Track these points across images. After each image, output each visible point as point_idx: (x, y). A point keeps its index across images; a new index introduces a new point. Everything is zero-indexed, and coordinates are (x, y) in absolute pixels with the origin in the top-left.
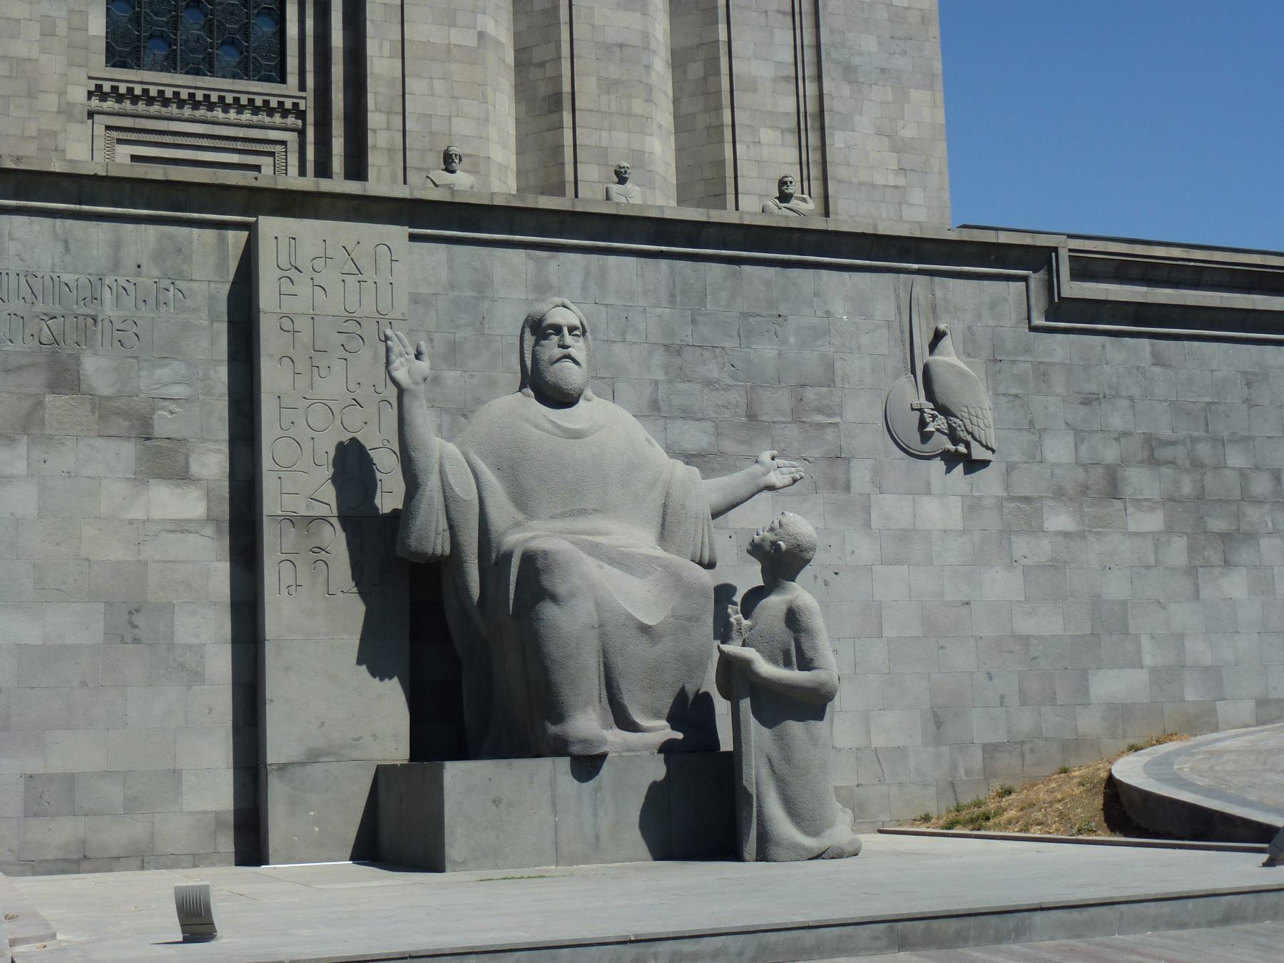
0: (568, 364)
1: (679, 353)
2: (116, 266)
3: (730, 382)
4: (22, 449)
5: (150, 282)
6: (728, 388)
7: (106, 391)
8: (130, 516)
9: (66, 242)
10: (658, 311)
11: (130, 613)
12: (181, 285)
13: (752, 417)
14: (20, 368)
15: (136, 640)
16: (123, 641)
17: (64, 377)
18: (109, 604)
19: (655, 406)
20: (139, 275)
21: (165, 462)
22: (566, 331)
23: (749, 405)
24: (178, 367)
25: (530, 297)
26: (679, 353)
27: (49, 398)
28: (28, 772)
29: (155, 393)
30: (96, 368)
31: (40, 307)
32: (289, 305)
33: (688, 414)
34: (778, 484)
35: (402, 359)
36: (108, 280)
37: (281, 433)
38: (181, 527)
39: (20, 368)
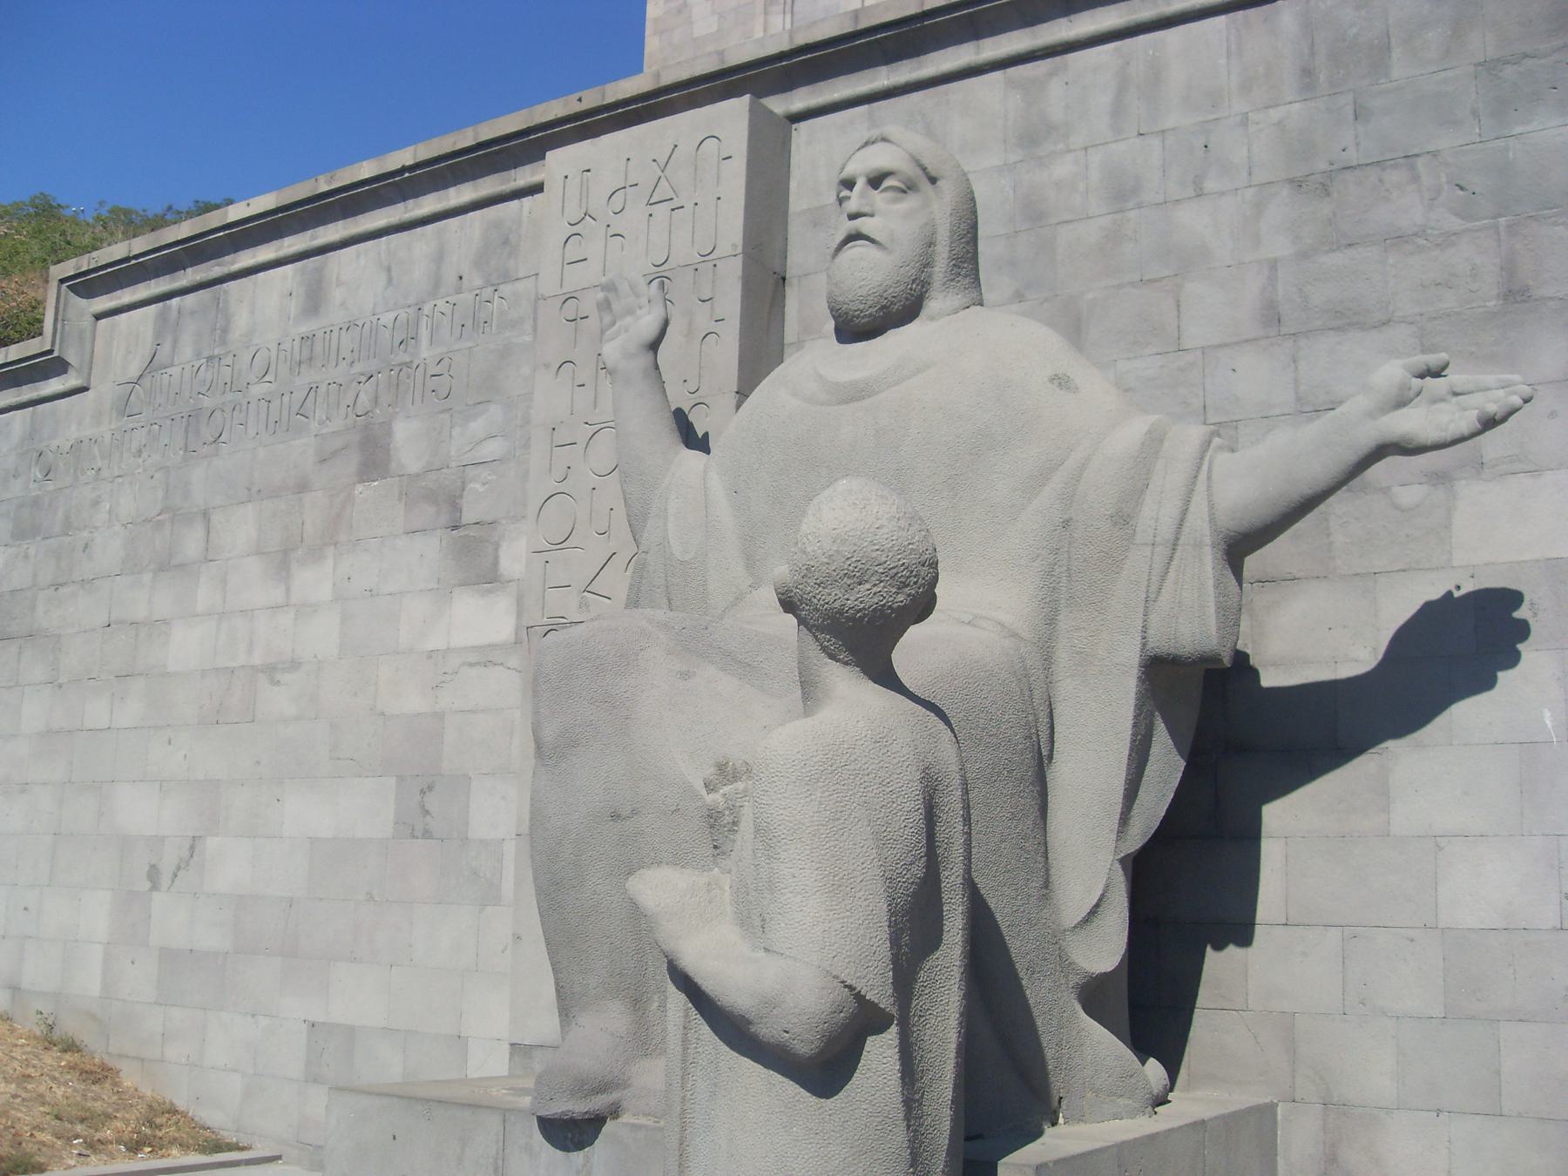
0: (858, 250)
1: (1326, 191)
2: (437, 283)
3: (1455, 224)
4: (330, 562)
5: (470, 296)
6: (1448, 240)
7: (414, 467)
8: (430, 647)
9: (389, 269)
10: (1275, 114)
11: (423, 792)
12: (506, 289)
13: (1515, 294)
14: (335, 454)
15: (427, 834)
16: (413, 837)
17: (373, 457)
18: (401, 779)
19: (1271, 316)
20: (459, 291)
21: (473, 560)
22: (861, 183)
23: (1509, 268)
24: (495, 412)
25: (1013, 158)
26: (1326, 191)
27: (360, 488)
28: (311, 1019)
29: (466, 460)
30: (408, 441)
31: (358, 368)
32: (577, 277)
33: (1348, 319)
34: (1431, 434)
35: (628, 320)
36: (427, 309)
37: (553, 487)
38: (485, 657)
39: (335, 454)
